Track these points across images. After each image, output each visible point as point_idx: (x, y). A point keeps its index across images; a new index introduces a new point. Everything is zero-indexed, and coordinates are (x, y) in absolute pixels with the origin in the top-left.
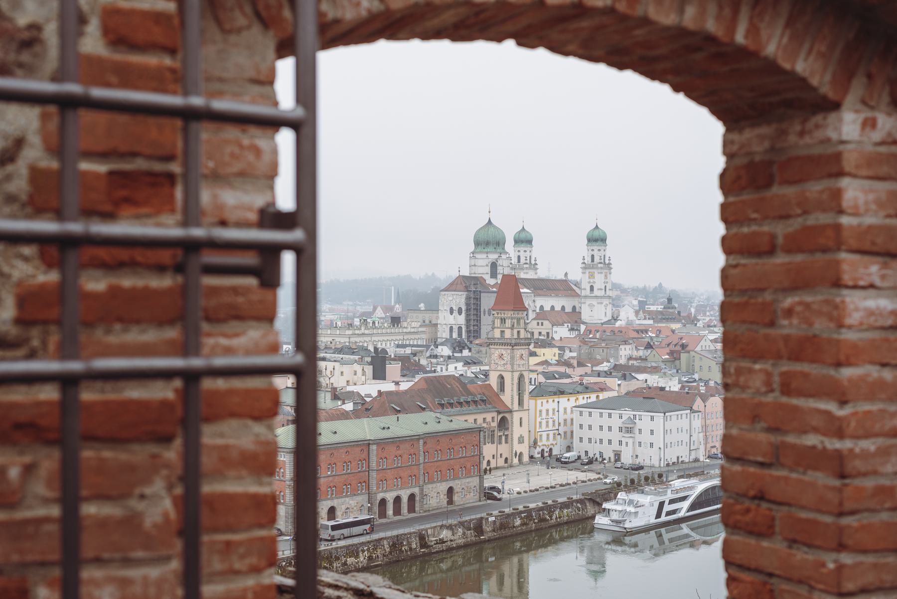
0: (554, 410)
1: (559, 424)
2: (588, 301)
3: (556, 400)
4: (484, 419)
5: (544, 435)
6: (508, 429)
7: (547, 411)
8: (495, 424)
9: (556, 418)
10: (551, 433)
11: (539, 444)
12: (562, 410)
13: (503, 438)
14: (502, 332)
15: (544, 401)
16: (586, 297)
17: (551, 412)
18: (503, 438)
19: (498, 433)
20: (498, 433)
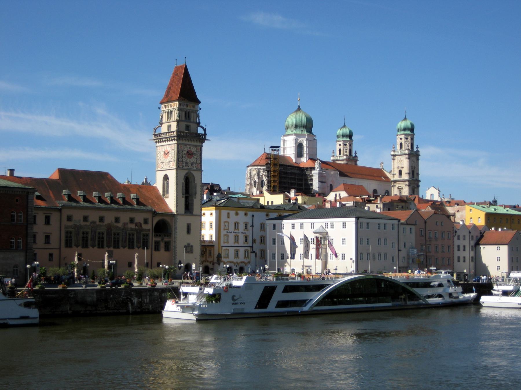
0: (246, 224)
1: (254, 241)
2: (397, 185)
3: (250, 214)
4: (132, 220)
5: (232, 251)
6: (169, 235)
7: (237, 225)
8: (149, 227)
9: (249, 233)
10: (242, 251)
11: (223, 259)
12: (257, 227)
13: (162, 245)
14: (169, 126)
15: (232, 213)
16: (395, 182)
17: (241, 227)
18: (162, 245)
19: (153, 239)
20: (153, 239)
